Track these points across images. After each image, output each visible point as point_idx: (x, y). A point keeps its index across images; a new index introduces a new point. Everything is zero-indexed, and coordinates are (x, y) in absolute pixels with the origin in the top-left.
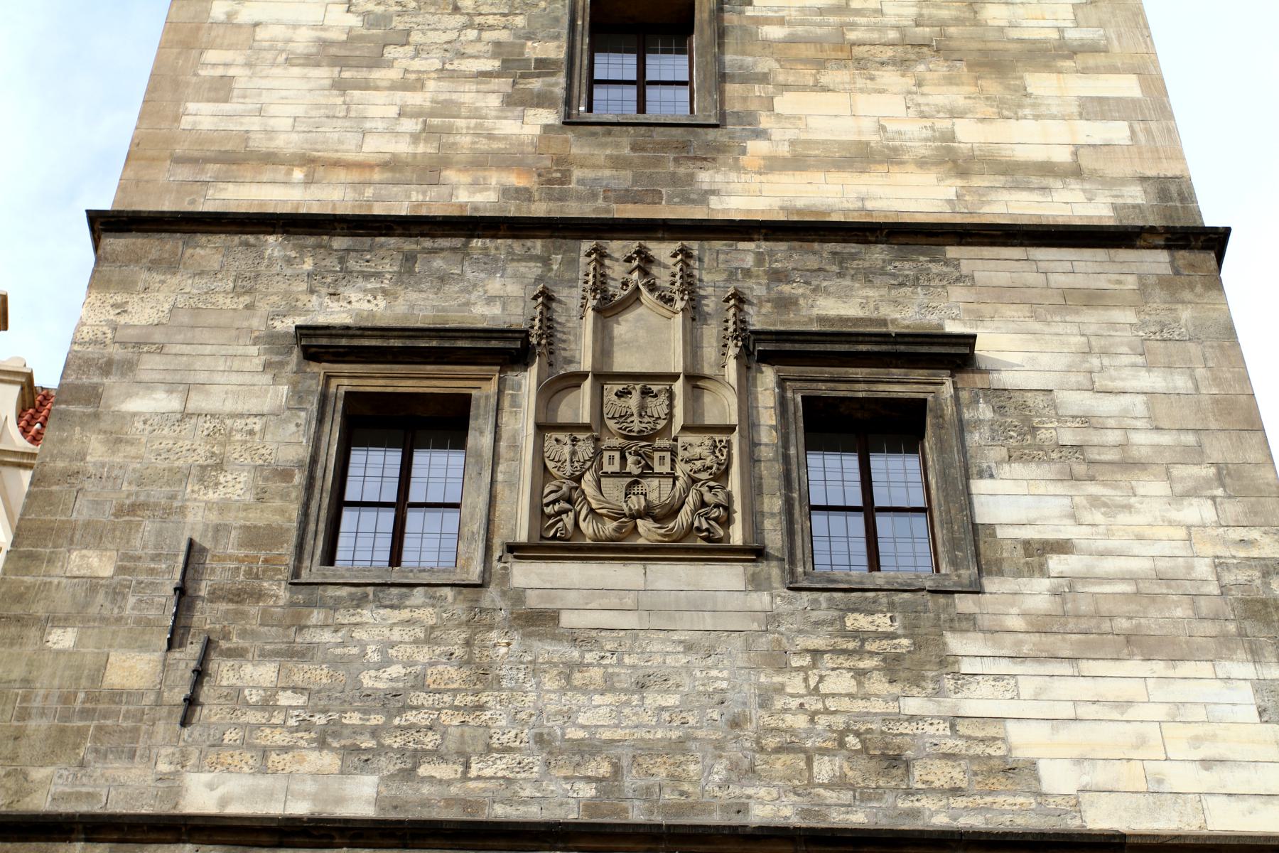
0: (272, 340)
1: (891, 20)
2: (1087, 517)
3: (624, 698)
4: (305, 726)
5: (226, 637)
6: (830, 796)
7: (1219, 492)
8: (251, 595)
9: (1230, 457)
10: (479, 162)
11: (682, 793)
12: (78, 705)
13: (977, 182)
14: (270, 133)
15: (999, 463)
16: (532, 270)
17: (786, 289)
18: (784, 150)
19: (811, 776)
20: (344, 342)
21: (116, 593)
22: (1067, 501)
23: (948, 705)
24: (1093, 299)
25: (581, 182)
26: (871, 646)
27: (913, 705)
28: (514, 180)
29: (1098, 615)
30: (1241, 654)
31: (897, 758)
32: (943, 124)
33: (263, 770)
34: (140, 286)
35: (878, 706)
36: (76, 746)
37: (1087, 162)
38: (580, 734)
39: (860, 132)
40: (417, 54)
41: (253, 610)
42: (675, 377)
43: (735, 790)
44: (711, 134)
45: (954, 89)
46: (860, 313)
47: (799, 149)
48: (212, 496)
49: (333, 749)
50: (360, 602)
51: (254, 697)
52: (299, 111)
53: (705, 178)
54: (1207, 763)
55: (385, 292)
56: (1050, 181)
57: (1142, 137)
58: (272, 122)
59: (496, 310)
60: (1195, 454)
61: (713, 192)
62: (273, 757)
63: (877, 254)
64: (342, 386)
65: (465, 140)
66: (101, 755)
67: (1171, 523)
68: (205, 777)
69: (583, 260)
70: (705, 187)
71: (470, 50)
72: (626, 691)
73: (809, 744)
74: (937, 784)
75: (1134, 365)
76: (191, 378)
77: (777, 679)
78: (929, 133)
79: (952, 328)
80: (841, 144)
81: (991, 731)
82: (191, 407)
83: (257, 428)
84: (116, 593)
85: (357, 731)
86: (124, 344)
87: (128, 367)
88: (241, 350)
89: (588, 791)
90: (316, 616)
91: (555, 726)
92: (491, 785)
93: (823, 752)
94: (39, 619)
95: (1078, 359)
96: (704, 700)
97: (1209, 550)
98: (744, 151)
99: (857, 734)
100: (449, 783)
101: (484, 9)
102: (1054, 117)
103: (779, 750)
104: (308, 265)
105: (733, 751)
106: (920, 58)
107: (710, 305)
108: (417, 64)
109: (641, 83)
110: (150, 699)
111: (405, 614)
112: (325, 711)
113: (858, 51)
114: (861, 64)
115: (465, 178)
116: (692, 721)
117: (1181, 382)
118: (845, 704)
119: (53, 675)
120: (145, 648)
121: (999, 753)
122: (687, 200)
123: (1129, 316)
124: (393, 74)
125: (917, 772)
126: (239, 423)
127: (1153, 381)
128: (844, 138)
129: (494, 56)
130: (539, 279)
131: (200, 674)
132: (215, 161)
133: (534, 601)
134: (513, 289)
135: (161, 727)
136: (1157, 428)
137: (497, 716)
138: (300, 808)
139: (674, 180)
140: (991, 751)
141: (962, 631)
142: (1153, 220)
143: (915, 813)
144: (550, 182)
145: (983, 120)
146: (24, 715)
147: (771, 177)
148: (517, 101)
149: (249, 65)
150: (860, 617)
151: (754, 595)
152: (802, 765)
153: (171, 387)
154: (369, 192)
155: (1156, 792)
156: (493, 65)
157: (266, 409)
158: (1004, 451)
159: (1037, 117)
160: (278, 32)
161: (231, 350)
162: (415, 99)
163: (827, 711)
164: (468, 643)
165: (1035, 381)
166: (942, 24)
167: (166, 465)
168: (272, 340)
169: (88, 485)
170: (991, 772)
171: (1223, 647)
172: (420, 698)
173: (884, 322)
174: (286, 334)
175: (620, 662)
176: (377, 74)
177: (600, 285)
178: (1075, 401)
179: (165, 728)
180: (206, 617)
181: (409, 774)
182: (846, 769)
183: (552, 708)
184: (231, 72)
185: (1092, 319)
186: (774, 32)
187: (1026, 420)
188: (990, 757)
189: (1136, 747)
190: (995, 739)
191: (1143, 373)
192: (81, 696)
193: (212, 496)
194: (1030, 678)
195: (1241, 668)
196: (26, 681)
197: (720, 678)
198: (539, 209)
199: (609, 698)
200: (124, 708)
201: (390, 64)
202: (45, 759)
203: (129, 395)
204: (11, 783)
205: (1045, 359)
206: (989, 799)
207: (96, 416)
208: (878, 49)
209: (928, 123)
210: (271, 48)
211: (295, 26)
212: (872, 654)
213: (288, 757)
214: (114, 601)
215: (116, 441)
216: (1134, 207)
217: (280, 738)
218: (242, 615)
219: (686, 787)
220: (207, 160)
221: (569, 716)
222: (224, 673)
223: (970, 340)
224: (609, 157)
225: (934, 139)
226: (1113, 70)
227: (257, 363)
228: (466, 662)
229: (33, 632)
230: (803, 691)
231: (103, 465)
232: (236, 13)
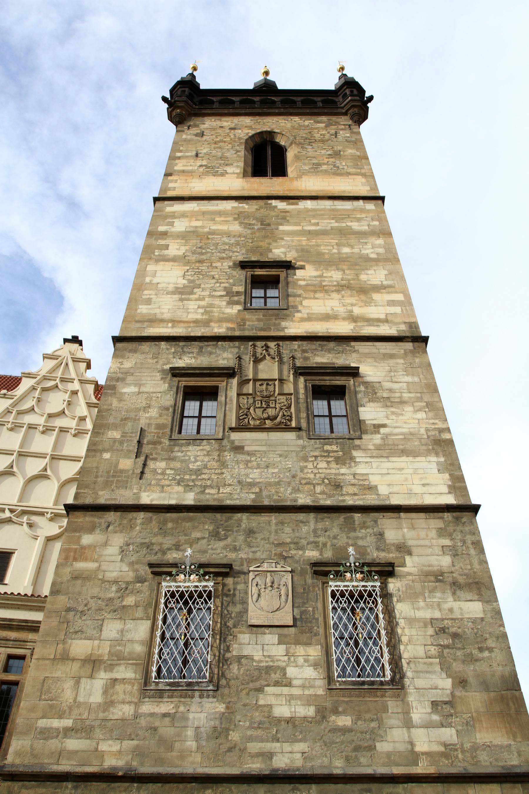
0: (163, 371)
1: (335, 279)
2: (391, 417)
3: (262, 470)
4: (174, 479)
5: (152, 454)
6: (320, 496)
7: (427, 410)
8: (158, 443)
9: (430, 400)
10: (220, 321)
11: (279, 496)
12: (111, 474)
13: (359, 324)
14: (162, 313)
15: (366, 402)
16: (236, 350)
17: (306, 355)
18: (305, 316)
19: (315, 491)
20: (183, 372)
21: (121, 443)
22: (385, 413)
23: (352, 470)
24: (392, 356)
25: (249, 325)
26: (331, 454)
27: (343, 471)
28: (230, 325)
29: (394, 445)
30: (433, 455)
31: (339, 485)
32: (350, 308)
33: (162, 491)
34: (127, 357)
35: (333, 471)
36: (111, 485)
37: (389, 318)
38: (251, 480)
39: (326, 311)
40: (203, 291)
41: (159, 447)
42: (276, 380)
43: (294, 495)
44: (285, 311)
45: (353, 298)
46: (327, 361)
47: (310, 315)
48: (147, 415)
49: (182, 486)
50: (189, 444)
51: (159, 471)
52: (170, 307)
53: (283, 324)
54: (424, 485)
55: (194, 357)
56: (379, 324)
57: (404, 311)
58: (162, 310)
59: (225, 362)
60: (420, 399)
61: (286, 328)
62: (165, 488)
63: (332, 345)
64: (184, 384)
65: (216, 314)
66: (118, 488)
67: (414, 419)
68: (146, 494)
69: (250, 347)
70: (283, 326)
71: (217, 289)
72: (262, 468)
73: (314, 482)
74: (350, 492)
75: (403, 375)
76: (141, 382)
77: (305, 464)
78: (345, 311)
79: (353, 365)
80: (322, 314)
81: (365, 477)
82: (141, 390)
83: (159, 396)
84: (121, 443)
85: (188, 480)
86: (122, 373)
87: (123, 380)
88: (154, 374)
89: (253, 496)
90: (177, 448)
91: (243, 478)
92: (226, 495)
93: (318, 484)
94: (100, 450)
95: (388, 373)
96: (285, 470)
97: (424, 426)
98: (294, 316)
99: (328, 479)
100: (214, 494)
101: (221, 278)
102: (380, 306)
103: (306, 484)
104: (173, 350)
105: (293, 484)
106: (343, 290)
107: (285, 360)
108: (203, 293)
109: (265, 298)
110: (131, 472)
111: (201, 448)
112: (179, 475)
113: (325, 287)
114: (326, 291)
115: (216, 325)
116: (281, 476)
117: (416, 379)
118: (324, 471)
119: (104, 466)
120: (129, 458)
121: (367, 483)
122: (278, 330)
123: (402, 361)
124: (196, 296)
125: (344, 489)
126: (154, 395)
127: (409, 379)
128: (322, 312)
129: (224, 291)
130: (237, 353)
131: (145, 465)
132: (147, 322)
133: (237, 443)
134: (230, 356)
135: (134, 480)
136: (410, 392)
137: (227, 475)
138: (173, 502)
139: (275, 325)
140: (365, 483)
141: (356, 450)
142: (408, 334)
143: (344, 501)
144: (240, 325)
145: (360, 307)
146: (97, 477)
147: (302, 323)
148: (231, 303)
149: (156, 295)
150: (328, 446)
151: (299, 441)
152: (312, 488)
153: (135, 385)
154: (190, 329)
155: (410, 493)
156: (224, 293)
157: (162, 391)
158: (368, 399)
159: (375, 306)
160: (164, 285)
161: (152, 374)
162: (202, 303)
163: (319, 473)
164: (219, 455)
165: (376, 379)
166: (349, 280)
167: (134, 407)
168: (163, 371)
169: (113, 413)
170: (365, 489)
171: (428, 453)
172: (206, 471)
173: (334, 364)
174: (167, 370)
175: (261, 460)
176: (192, 297)
177: (254, 354)
178: (387, 385)
179: (135, 480)
180: (146, 449)
181: (203, 492)
182: (325, 489)
183: (242, 473)
184: (151, 297)
185: (392, 362)
186: (302, 283)
187: (374, 390)
188: (365, 485)
189: (405, 481)
190: (366, 480)
191: (406, 377)
192: (112, 471)
193: (147, 415)
194: (375, 462)
195: (433, 459)
196: (97, 468)
197: (289, 464)
198: (237, 333)
199: (258, 470)
200: (124, 475)
201: (195, 294)
202: (103, 489)
203: (124, 387)
204: (93, 496)
205: (379, 373)
206: (364, 496)
207: (115, 393)
208: (330, 287)
209: (345, 308)
210: (162, 290)
211: (169, 284)
212: (331, 457)
213: (169, 488)
214: (120, 445)
215: (120, 400)
216: (403, 330)
217: (167, 482)
218: (156, 448)
219: (280, 495)
220: (145, 321)
221: (247, 475)
222: (151, 465)
223: (358, 368)
224: (256, 318)
225: (347, 312)
226: (396, 292)
227: (159, 378)
228: (219, 461)
229: (99, 454)
230: (312, 467)
231: (117, 407)
232: (152, 280)
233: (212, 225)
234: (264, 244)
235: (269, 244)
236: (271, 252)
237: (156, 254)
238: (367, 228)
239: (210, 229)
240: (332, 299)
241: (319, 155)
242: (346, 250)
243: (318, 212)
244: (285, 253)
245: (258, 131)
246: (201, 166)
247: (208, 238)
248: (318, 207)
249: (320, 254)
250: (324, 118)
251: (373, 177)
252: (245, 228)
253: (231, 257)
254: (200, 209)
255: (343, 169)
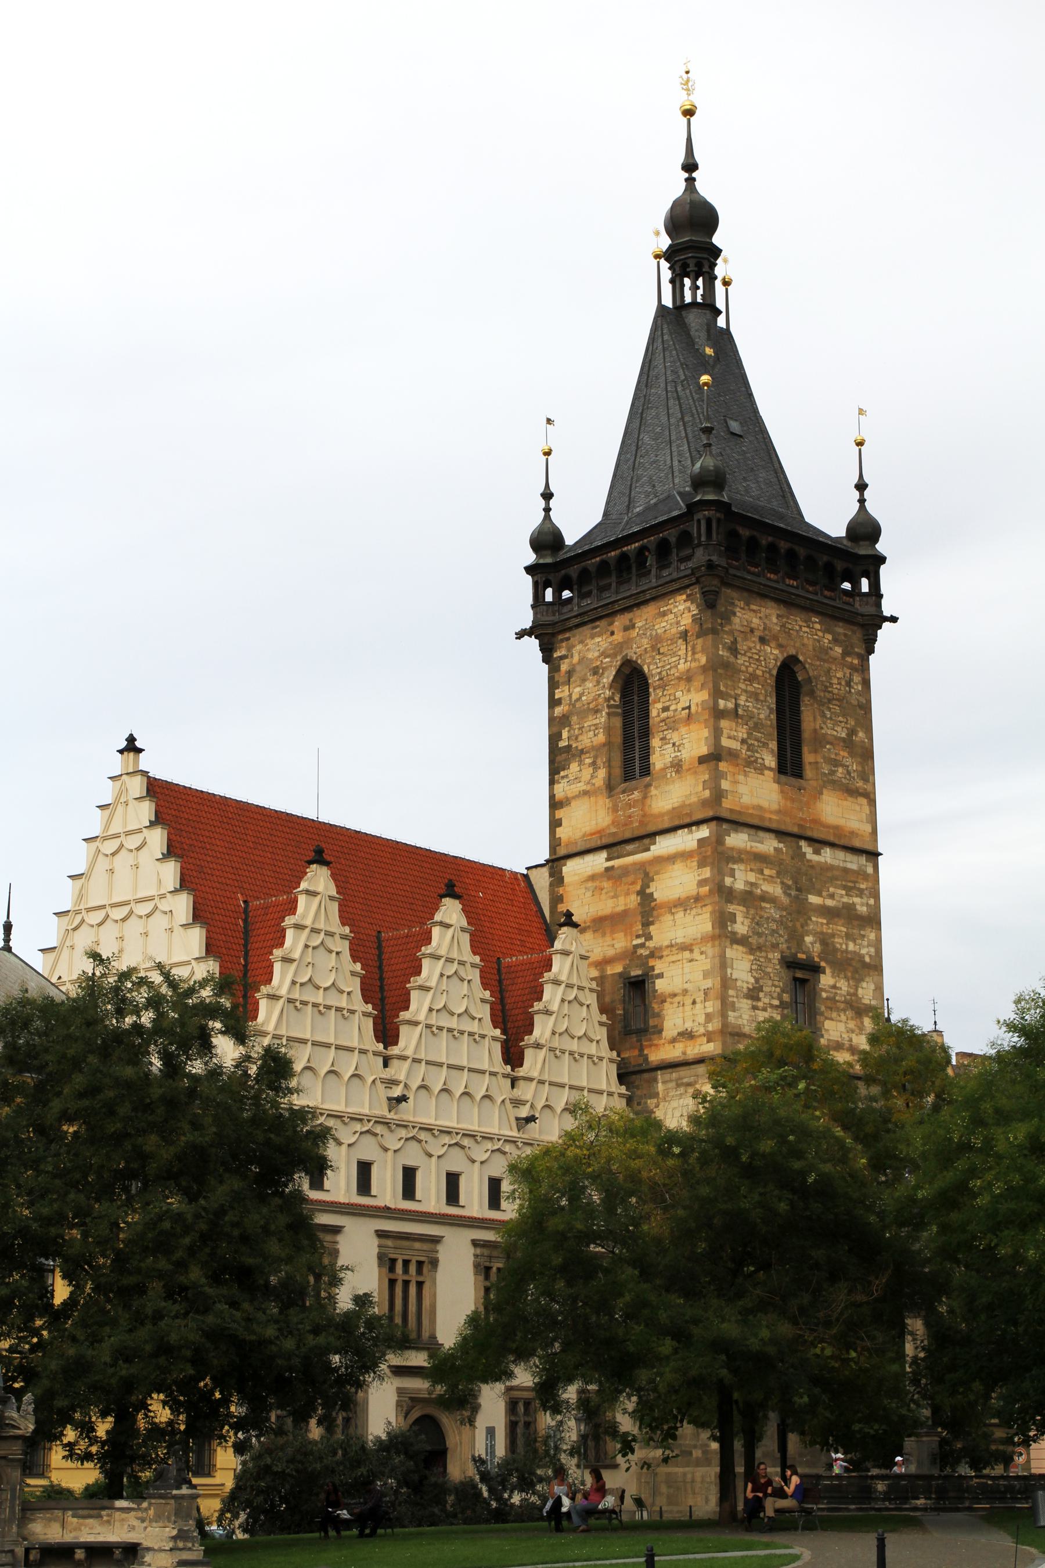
101: (776, 978)
114: (838, 1010)
149: (737, 997)
211: (743, 981)
233: (761, 882)
234: (798, 925)
235: (802, 927)
236: (804, 941)
237: (729, 928)
238: (865, 909)
239: (762, 890)
240: (841, 1021)
241: (836, 738)
242: (851, 947)
243: (836, 873)
244: (812, 944)
245: (785, 655)
246: (743, 741)
247: (762, 908)
248: (836, 863)
249: (835, 950)
250: (840, 629)
251: (875, 801)
252: (785, 893)
253: (778, 944)
254: (751, 847)
255: (854, 778)
